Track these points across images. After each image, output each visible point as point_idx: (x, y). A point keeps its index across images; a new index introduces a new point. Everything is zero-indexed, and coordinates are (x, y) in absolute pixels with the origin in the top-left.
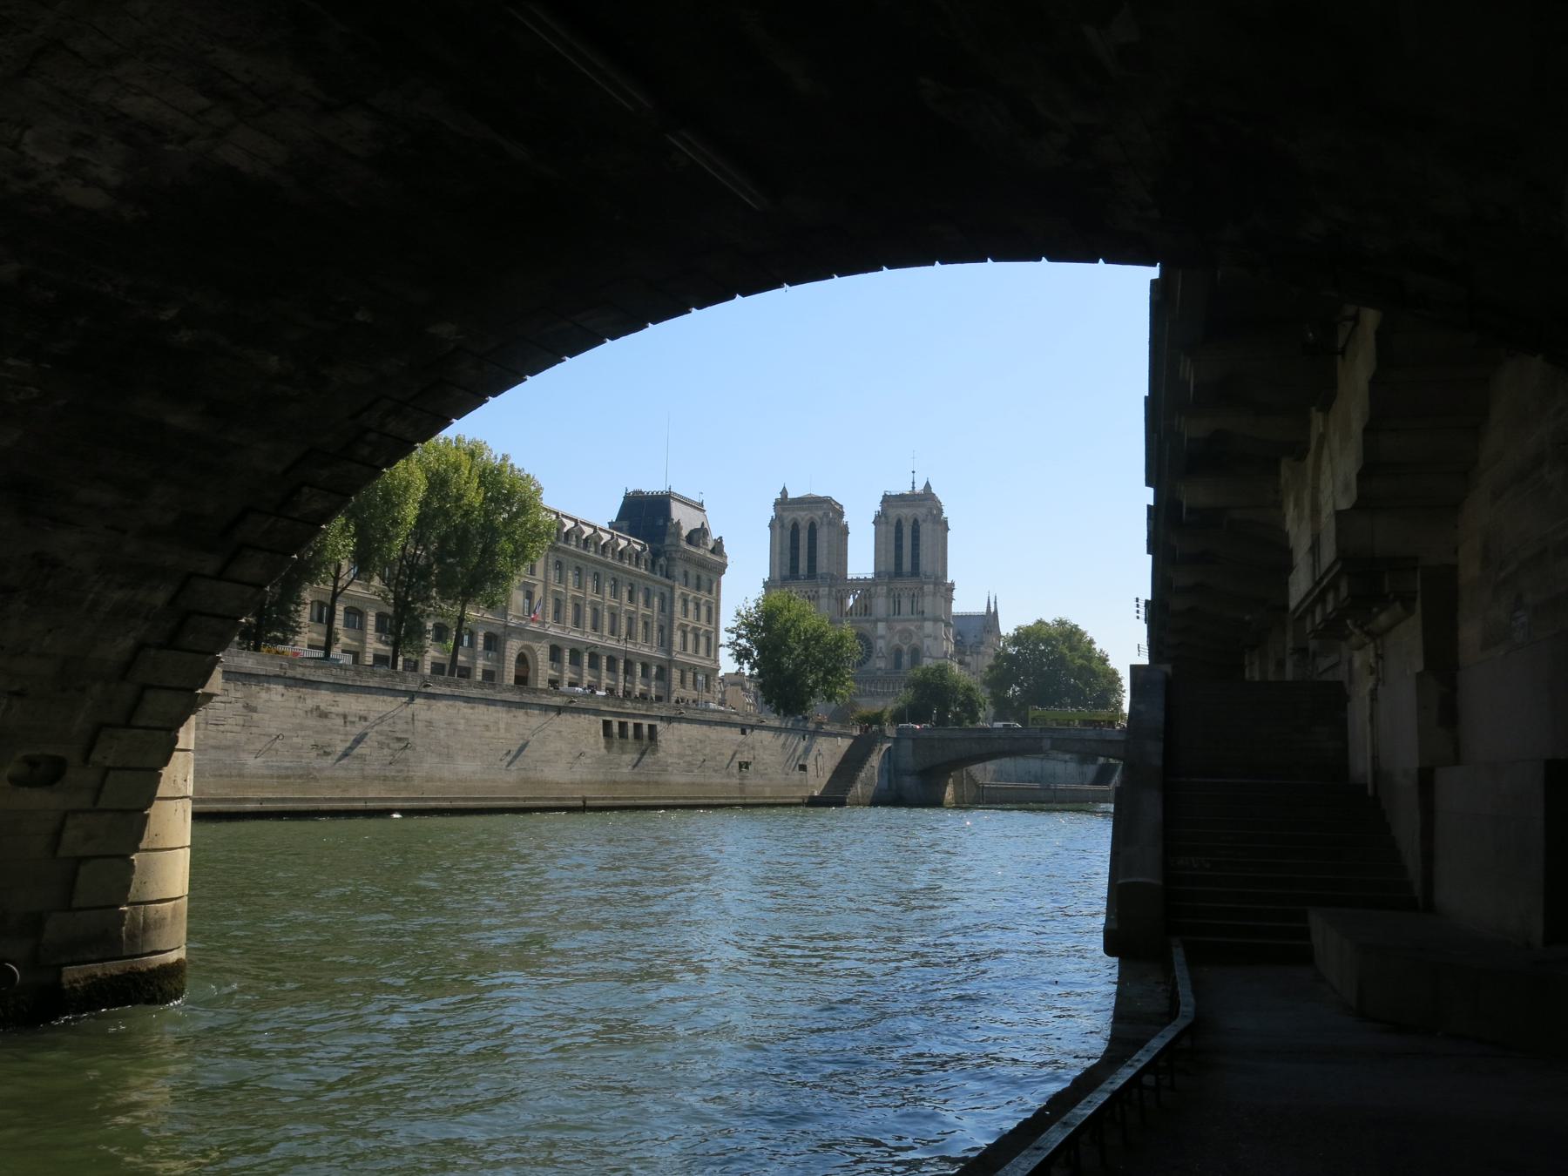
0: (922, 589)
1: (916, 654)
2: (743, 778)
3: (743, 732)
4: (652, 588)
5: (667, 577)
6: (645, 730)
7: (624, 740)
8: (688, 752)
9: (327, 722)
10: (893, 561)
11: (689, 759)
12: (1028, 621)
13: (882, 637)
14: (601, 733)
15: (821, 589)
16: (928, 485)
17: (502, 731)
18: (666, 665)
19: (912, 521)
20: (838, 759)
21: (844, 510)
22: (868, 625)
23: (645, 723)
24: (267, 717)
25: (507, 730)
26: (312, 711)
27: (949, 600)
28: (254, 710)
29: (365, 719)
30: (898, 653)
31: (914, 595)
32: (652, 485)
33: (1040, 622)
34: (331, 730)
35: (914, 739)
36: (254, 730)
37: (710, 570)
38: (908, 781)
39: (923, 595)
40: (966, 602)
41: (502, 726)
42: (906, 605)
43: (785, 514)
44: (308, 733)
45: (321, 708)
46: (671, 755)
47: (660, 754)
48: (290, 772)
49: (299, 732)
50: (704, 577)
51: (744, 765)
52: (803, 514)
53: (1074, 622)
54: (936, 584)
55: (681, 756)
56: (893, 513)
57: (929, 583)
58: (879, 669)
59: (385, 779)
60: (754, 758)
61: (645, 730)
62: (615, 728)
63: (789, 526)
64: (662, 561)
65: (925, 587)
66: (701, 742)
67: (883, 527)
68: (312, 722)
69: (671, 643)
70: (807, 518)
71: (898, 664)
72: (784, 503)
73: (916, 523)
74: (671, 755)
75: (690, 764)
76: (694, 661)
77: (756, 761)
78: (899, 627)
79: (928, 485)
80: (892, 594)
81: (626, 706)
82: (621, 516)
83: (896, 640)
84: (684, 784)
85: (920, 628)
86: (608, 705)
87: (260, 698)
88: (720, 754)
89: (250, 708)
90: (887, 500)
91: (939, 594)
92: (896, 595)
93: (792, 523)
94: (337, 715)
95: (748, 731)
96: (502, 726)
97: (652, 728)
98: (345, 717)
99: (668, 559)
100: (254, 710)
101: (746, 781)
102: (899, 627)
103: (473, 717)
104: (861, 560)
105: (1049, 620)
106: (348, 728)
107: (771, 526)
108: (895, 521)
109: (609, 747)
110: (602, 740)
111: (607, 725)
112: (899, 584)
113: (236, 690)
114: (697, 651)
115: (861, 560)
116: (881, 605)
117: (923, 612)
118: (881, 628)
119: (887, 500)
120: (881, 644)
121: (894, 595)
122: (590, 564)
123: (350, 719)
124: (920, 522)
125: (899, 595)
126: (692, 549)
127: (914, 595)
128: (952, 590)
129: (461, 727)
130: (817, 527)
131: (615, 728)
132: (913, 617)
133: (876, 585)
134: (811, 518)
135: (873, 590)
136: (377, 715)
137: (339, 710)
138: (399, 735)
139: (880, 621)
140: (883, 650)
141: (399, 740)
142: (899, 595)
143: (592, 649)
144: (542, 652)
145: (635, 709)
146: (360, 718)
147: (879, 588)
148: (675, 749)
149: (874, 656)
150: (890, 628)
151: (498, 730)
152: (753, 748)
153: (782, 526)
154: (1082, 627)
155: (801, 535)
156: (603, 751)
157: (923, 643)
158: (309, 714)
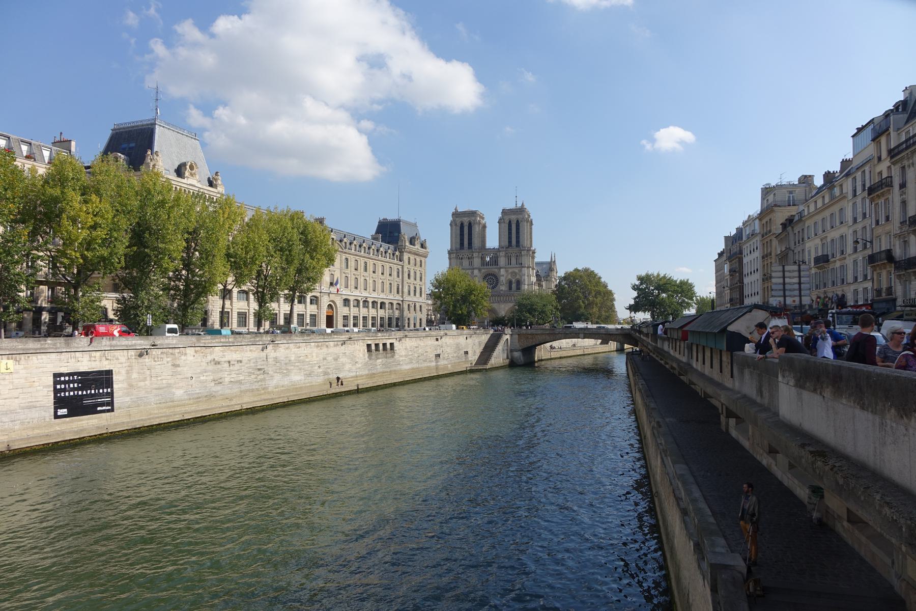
0: (521, 253)
1: (519, 283)
2: (437, 362)
3: (437, 340)
4: (393, 267)
5: (400, 261)
6: (388, 346)
7: (377, 352)
8: (410, 353)
9: (219, 366)
11: (410, 357)
12: (570, 269)
13: (503, 276)
14: (366, 351)
15: (474, 254)
17: (315, 357)
18: (401, 302)
19: (515, 222)
20: (483, 346)
22: (496, 270)
23: (388, 342)
24: (185, 369)
25: (317, 357)
26: (211, 362)
27: (533, 258)
28: (178, 366)
29: (241, 362)
30: (510, 283)
32: (391, 216)
33: (576, 270)
34: (221, 370)
36: (178, 376)
37: (421, 256)
38: (517, 354)
40: (541, 256)
41: (314, 354)
42: (513, 261)
43: (457, 219)
44: (208, 374)
45: (216, 359)
46: (401, 356)
47: (397, 356)
48: (200, 395)
49: (205, 374)
50: (418, 260)
51: (438, 356)
52: (465, 219)
53: (592, 269)
55: (406, 356)
56: (507, 219)
57: (524, 250)
58: (502, 290)
59: (253, 390)
61: (388, 346)
62: (373, 347)
63: (459, 224)
64: (397, 253)
65: (522, 252)
66: (416, 347)
67: (503, 225)
68: (211, 367)
69: (403, 292)
71: (510, 288)
72: (456, 214)
73: (518, 221)
74: (401, 356)
75: (411, 359)
76: (415, 299)
78: (510, 271)
82: (378, 232)
83: (509, 277)
85: (520, 271)
87: (181, 359)
89: (175, 366)
90: (504, 212)
94: (225, 362)
96: (314, 354)
97: (392, 344)
98: (229, 362)
99: (400, 252)
100: (178, 366)
101: (439, 363)
102: (510, 271)
103: (299, 352)
104: (493, 240)
105: (580, 268)
106: (231, 368)
107: (451, 225)
109: (370, 357)
110: (367, 355)
111: (369, 346)
112: (510, 250)
113: (167, 357)
114: (415, 295)
115: (493, 240)
116: (502, 261)
117: (521, 264)
118: (503, 271)
119: (504, 212)
120: (503, 279)
122: (362, 258)
123: (232, 363)
126: (412, 246)
128: (535, 253)
129: (293, 359)
131: (373, 347)
132: (518, 266)
133: (500, 251)
135: (498, 254)
136: (247, 359)
137: (227, 359)
138: (258, 367)
139: (502, 268)
140: (504, 282)
141: (259, 369)
143: (364, 299)
144: (339, 302)
146: (238, 361)
148: (403, 353)
149: (499, 285)
150: (507, 271)
151: (313, 356)
152: (442, 347)
153: (456, 225)
154: (596, 272)
156: (367, 359)
157: (521, 277)
158: (209, 364)
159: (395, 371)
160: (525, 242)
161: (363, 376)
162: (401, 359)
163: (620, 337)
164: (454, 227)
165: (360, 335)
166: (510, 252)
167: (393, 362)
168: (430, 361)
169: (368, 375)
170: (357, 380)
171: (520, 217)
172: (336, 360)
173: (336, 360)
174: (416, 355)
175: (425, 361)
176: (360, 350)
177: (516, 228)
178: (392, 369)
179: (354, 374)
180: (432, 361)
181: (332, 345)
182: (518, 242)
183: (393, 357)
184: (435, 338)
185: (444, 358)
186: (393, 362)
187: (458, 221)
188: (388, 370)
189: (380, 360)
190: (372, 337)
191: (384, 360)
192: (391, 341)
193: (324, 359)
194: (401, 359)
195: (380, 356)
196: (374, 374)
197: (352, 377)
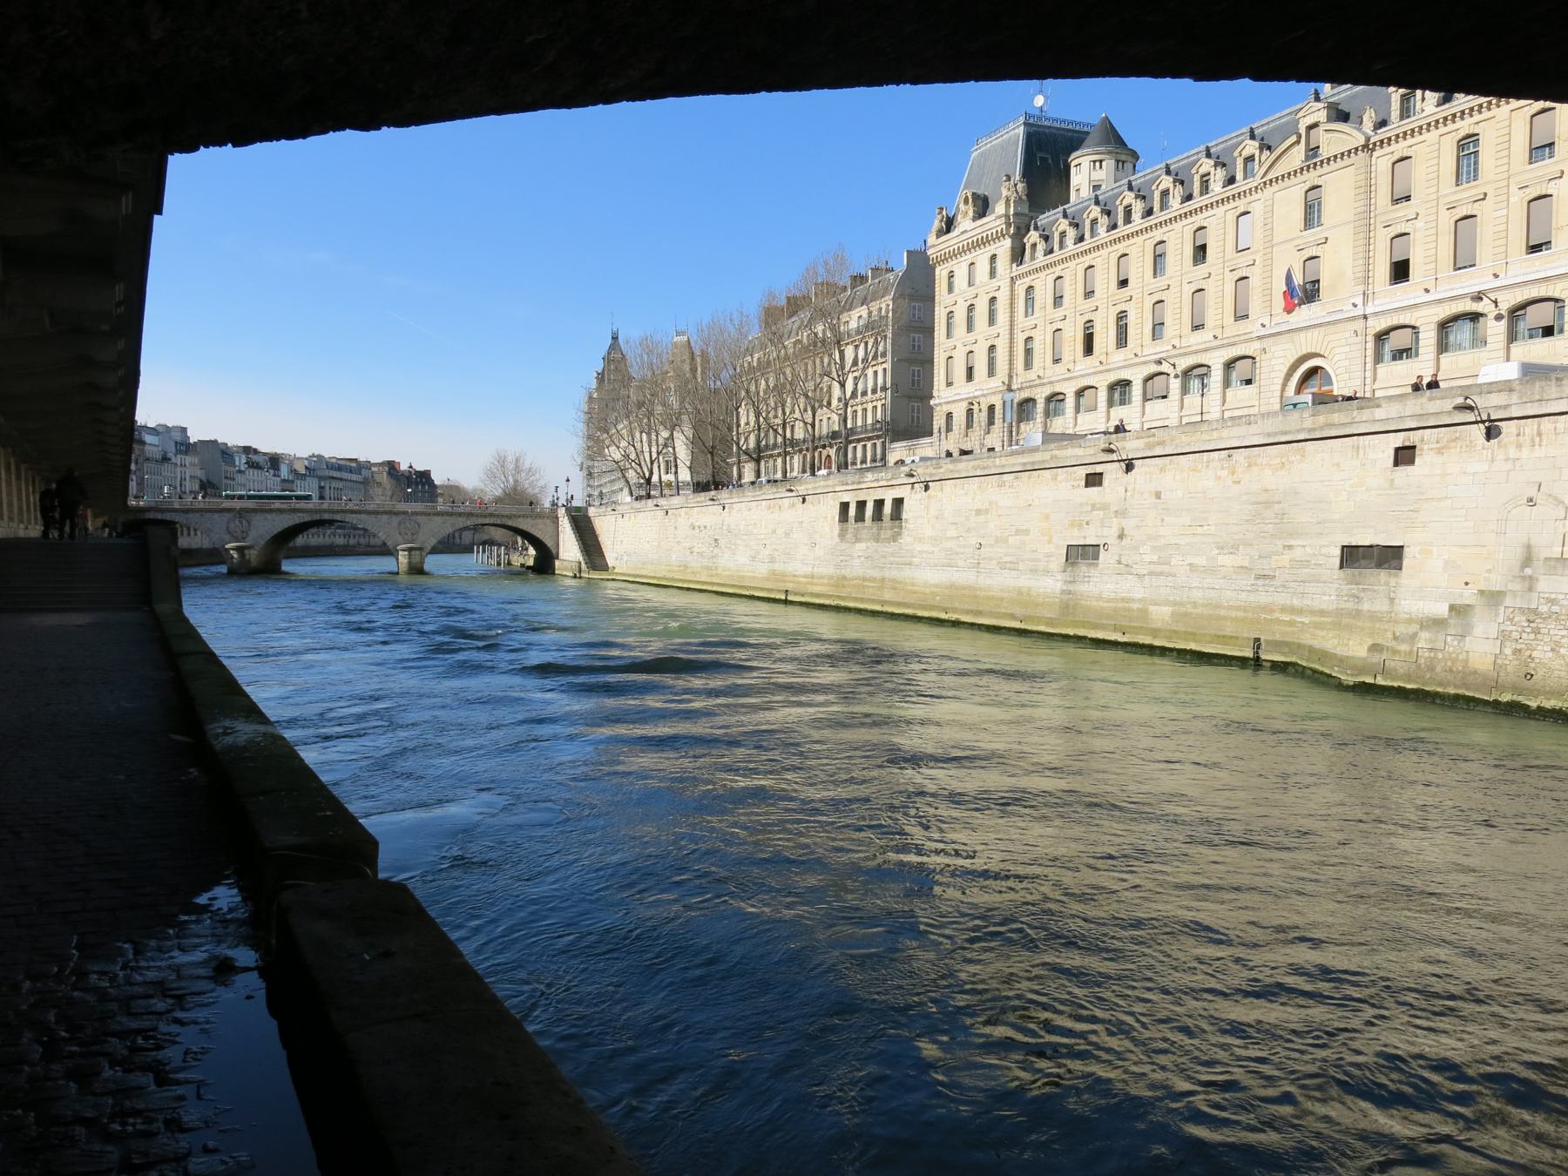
7: (859, 524)
8: (952, 532)
23: (889, 497)
47: (906, 539)
60: (1121, 536)
62: (852, 511)
66: (978, 512)
74: (920, 540)
77: (1126, 541)
81: (866, 480)
84: (936, 586)
86: (847, 484)
88: (1018, 532)
95: (1112, 473)
97: (898, 503)
109: (842, 535)
110: (837, 527)
131: (852, 511)
145: (877, 480)
156: (837, 539)
159: (894, 581)
161: (823, 578)
162: (918, 547)
165: (830, 482)
167: (892, 555)
168: (1034, 571)
169: (831, 578)
170: (812, 584)
172: (787, 535)
173: (787, 535)
174: (974, 541)
175: (1012, 566)
176: (826, 518)
178: (887, 574)
179: (808, 570)
180: (1047, 572)
181: (786, 506)
183: (895, 538)
184: (1083, 471)
185: (1125, 568)
186: (892, 555)
188: (877, 574)
189: (862, 546)
190: (853, 483)
191: (872, 544)
192: (897, 493)
193: (774, 532)
194: (918, 547)
195: (864, 534)
196: (844, 578)
197: (805, 577)
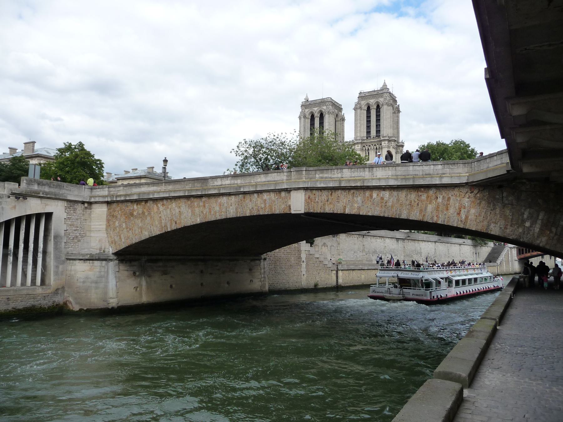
10: (365, 131)
16: (385, 85)
19: (375, 107)
21: (342, 107)
31: (377, 149)
35: (108, 203)
39: (382, 148)
43: (307, 110)
52: (316, 109)
54: (389, 141)
57: (384, 140)
65: (383, 143)
67: (359, 111)
70: (318, 111)
72: (306, 105)
79: (385, 85)
80: (364, 149)
91: (391, 147)
92: (367, 149)
93: (311, 115)
105: (447, 142)
107: (300, 118)
108: (366, 108)
121: (366, 149)
124: (380, 106)
125: (368, 149)
127: (377, 149)
130: (324, 115)
134: (321, 111)
142: (368, 149)
147: (356, 146)
153: (305, 117)
155: (316, 120)
160: (386, 131)
163: (466, 201)
164: (302, 119)
166: (368, 144)
171: (381, 100)
177: (377, 115)
182: (378, 131)
187: (307, 111)
